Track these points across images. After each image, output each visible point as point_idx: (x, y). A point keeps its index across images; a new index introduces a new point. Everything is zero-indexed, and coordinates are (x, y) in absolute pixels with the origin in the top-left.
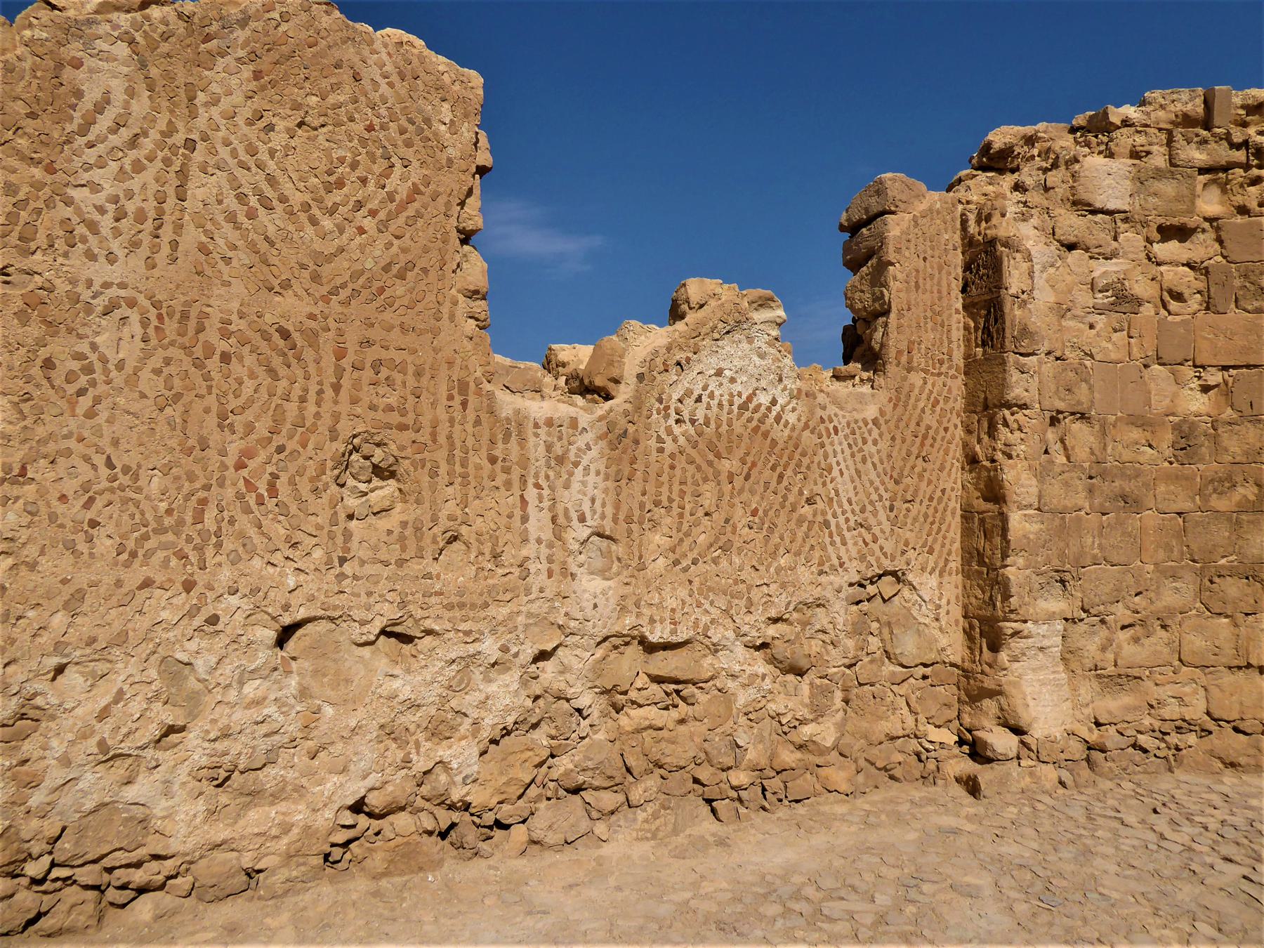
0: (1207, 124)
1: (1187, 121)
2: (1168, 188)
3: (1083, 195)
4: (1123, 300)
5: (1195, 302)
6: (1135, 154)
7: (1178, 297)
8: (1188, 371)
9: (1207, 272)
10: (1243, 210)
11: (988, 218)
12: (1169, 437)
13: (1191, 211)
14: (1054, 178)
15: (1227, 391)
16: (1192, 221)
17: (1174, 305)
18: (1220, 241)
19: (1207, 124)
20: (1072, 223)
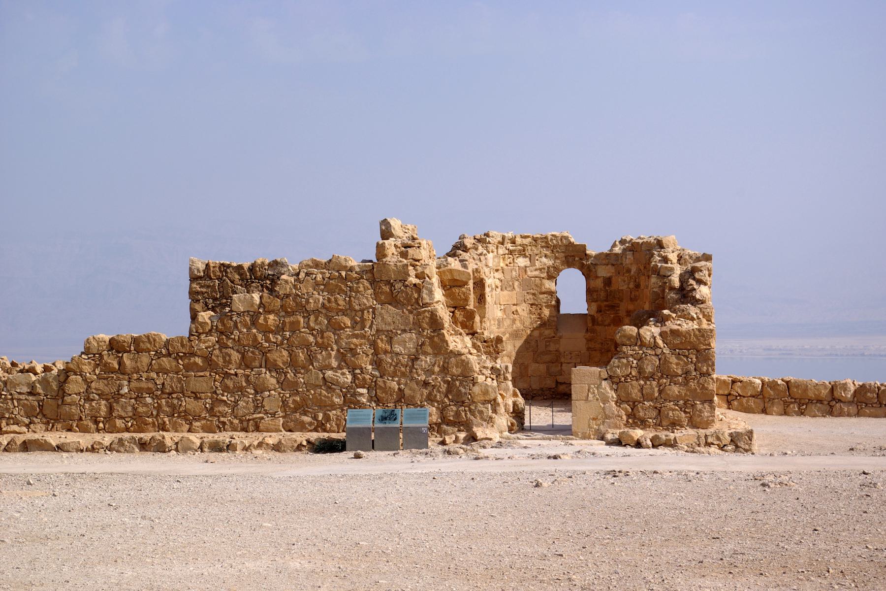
0: (502, 243)
1: (499, 242)
2: (496, 260)
3: (488, 264)
4: (492, 289)
5: (500, 288)
6: (493, 252)
7: (497, 287)
8: (499, 306)
9: (501, 281)
10: (507, 265)
11: (480, 272)
12: (497, 322)
13: (499, 266)
14: (482, 258)
15: (504, 310)
16: (500, 268)
17: (497, 289)
18: (503, 272)
19: (502, 243)
20: (487, 270)
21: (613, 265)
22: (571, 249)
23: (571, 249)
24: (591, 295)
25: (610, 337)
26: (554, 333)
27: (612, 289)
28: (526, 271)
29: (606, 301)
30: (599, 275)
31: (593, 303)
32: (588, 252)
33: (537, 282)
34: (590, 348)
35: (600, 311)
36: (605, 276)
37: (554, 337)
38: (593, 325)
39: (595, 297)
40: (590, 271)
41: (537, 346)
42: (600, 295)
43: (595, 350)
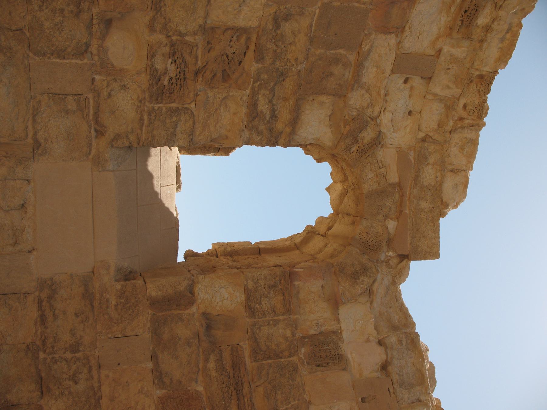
21: (384, 367)
22: (424, 205)
23: (424, 205)
24: (272, 287)
25: (106, 390)
26: (117, 137)
27: (304, 371)
28: (385, 30)
29: (256, 352)
30: (343, 311)
31: (241, 297)
32: (414, 265)
33: (337, 70)
34: (50, 298)
35: (209, 328)
36: (345, 335)
37: (100, 133)
38: (155, 303)
39: (266, 304)
40: (355, 277)
41: (61, 53)
42: (276, 323)
43: (43, 319)
